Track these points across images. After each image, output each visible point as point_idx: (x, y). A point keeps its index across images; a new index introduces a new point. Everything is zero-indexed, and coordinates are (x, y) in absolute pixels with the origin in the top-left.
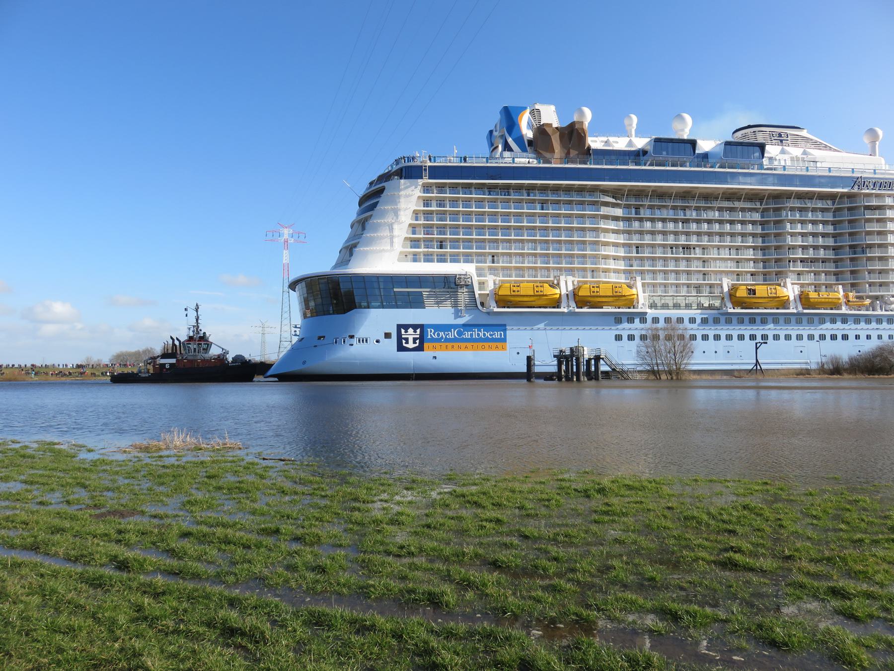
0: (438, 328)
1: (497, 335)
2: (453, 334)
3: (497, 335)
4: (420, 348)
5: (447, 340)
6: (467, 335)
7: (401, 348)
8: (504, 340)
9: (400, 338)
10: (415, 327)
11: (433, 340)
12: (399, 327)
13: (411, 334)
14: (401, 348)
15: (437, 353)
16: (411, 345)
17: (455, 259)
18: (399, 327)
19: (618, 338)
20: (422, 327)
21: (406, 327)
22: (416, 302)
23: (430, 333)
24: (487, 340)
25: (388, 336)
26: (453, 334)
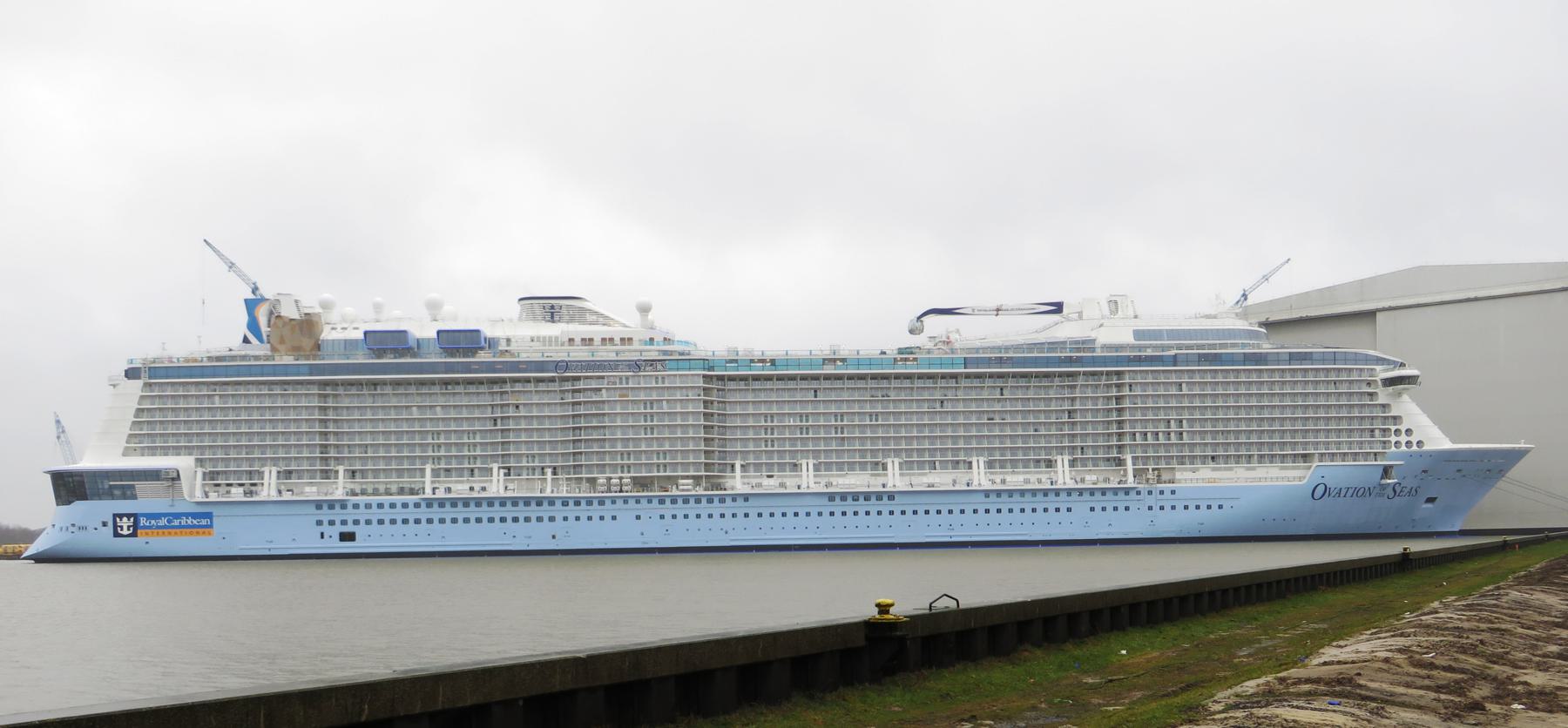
0: (150, 516)
1: (204, 522)
2: (163, 522)
3: (204, 522)
4: (134, 535)
5: (158, 527)
6: (176, 522)
7: (116, 535)
8: (211, 526)
9: (115, 526)
10: (129, 516)
11: (145, 527)
12: (115, 516)
13: (125, 523)
14: (116, 535)
15: (149, 539)
16: (125, 532)
17: (166, 451)
18: (115, 516)
19: (319, 523)
20: (135, 516)
21: (121, 516)
22: (128, 494)
23: (143, 521)
24: (194, 526)
25: (105, 524)
26: (163, 522)
